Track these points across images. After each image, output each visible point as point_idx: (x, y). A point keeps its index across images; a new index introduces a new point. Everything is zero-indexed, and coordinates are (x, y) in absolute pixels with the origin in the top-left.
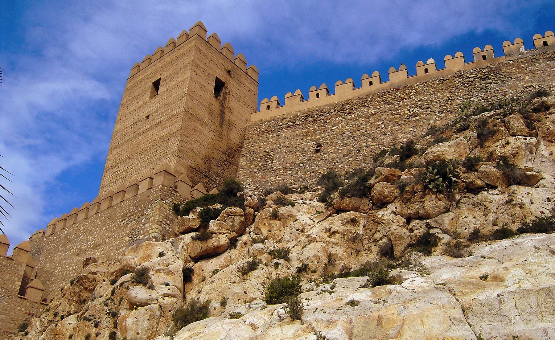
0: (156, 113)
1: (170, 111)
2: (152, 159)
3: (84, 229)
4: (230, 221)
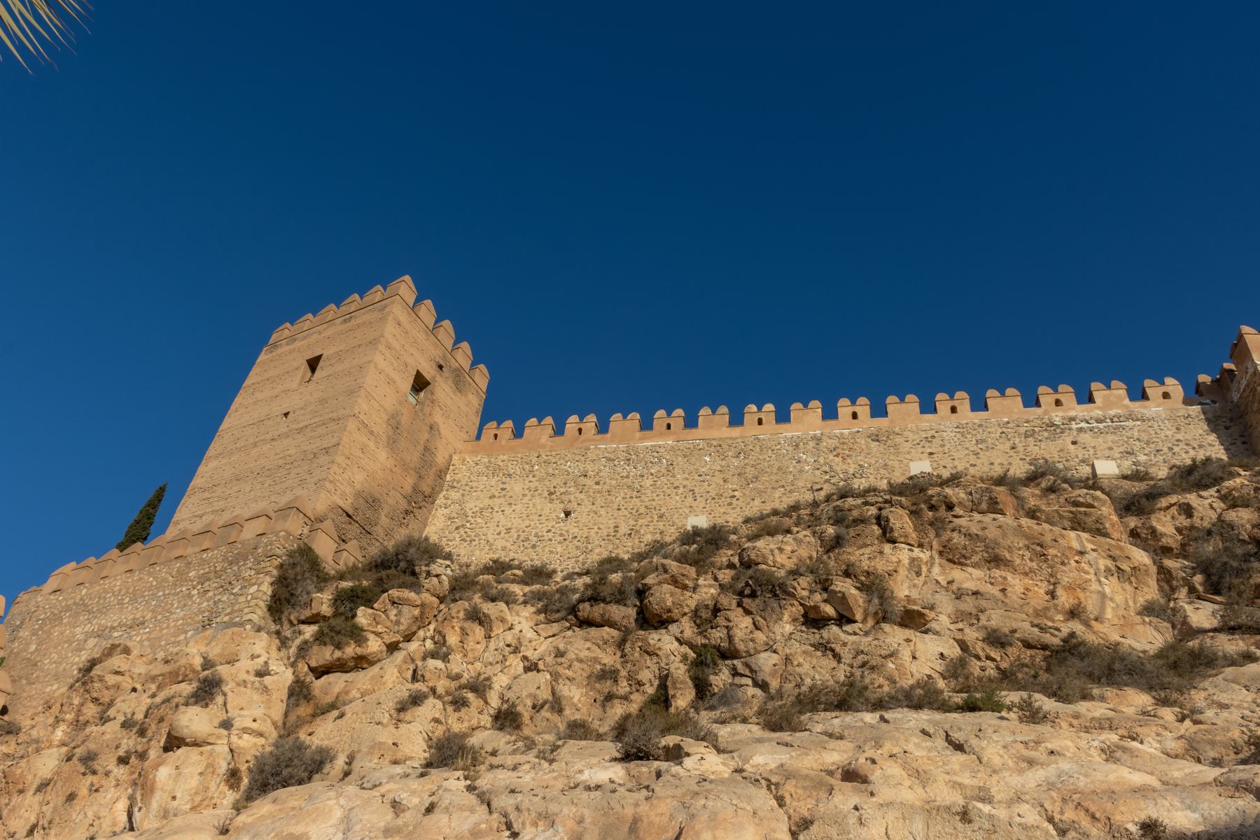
2: (277, 487)
3: (120, 590)
4: (393, 613)
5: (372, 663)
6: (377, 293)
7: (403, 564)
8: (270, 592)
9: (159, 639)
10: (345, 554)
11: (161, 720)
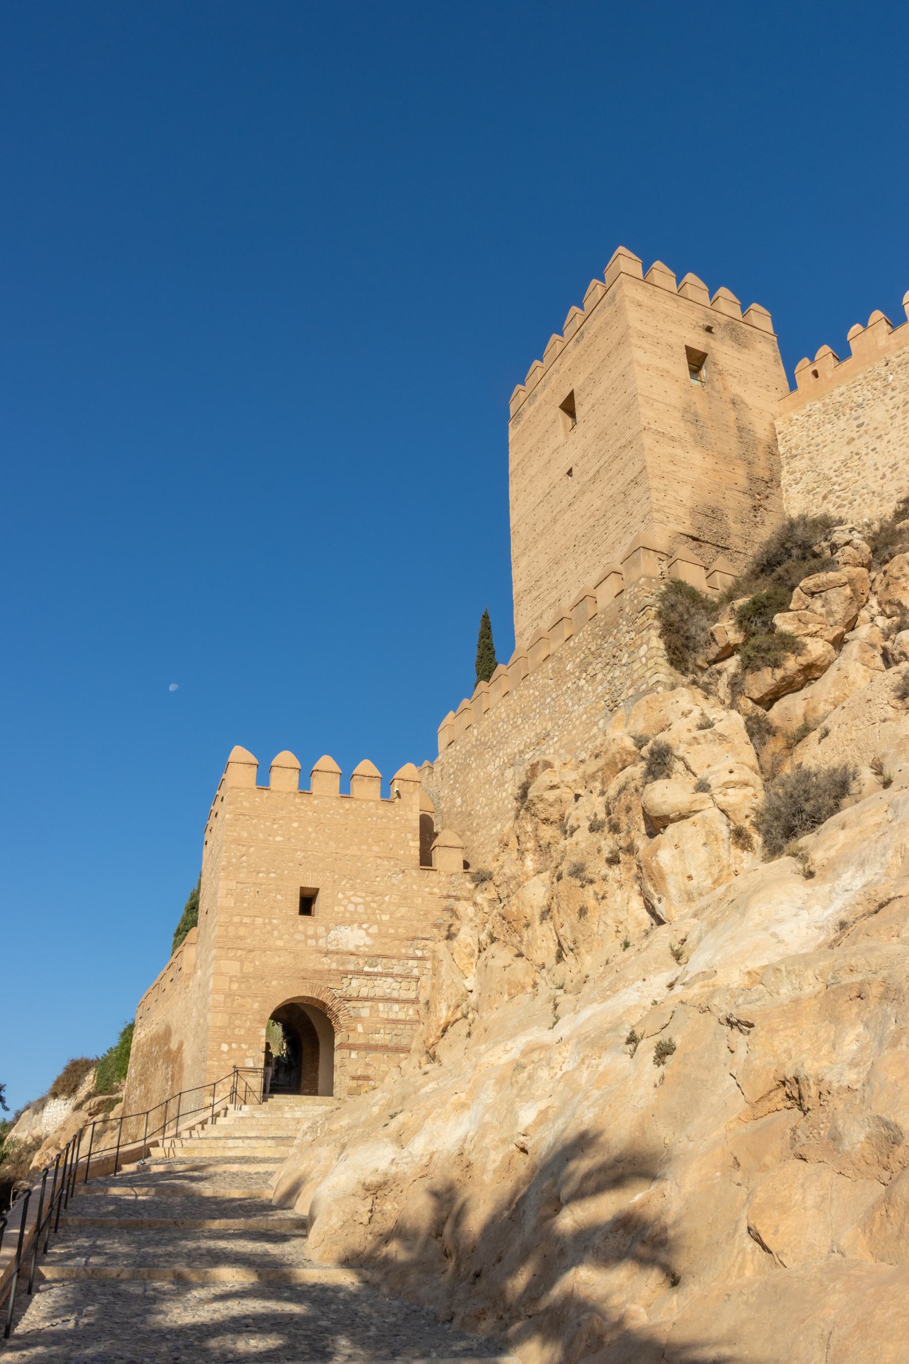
0: (585, 459)
1: (611, 442)
3: (508, 715)
4: (817, 604)
5: (824, 669)
6: (595, 289)
7: (795, 552)
8: (662, 646)
9: (573, 741)
10: (717, 574)
11: (628, 809)
